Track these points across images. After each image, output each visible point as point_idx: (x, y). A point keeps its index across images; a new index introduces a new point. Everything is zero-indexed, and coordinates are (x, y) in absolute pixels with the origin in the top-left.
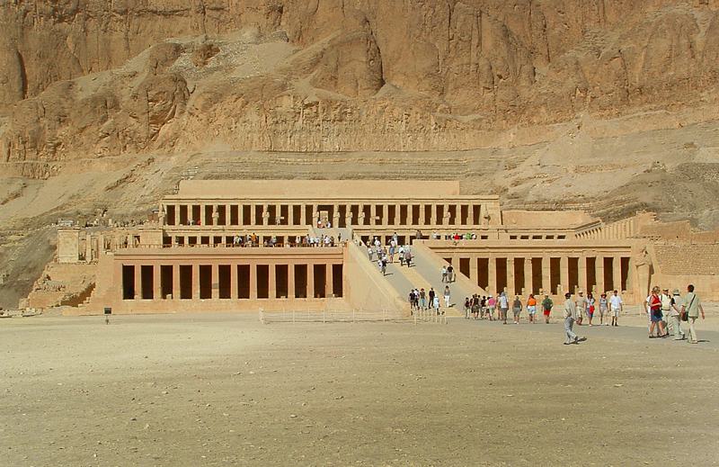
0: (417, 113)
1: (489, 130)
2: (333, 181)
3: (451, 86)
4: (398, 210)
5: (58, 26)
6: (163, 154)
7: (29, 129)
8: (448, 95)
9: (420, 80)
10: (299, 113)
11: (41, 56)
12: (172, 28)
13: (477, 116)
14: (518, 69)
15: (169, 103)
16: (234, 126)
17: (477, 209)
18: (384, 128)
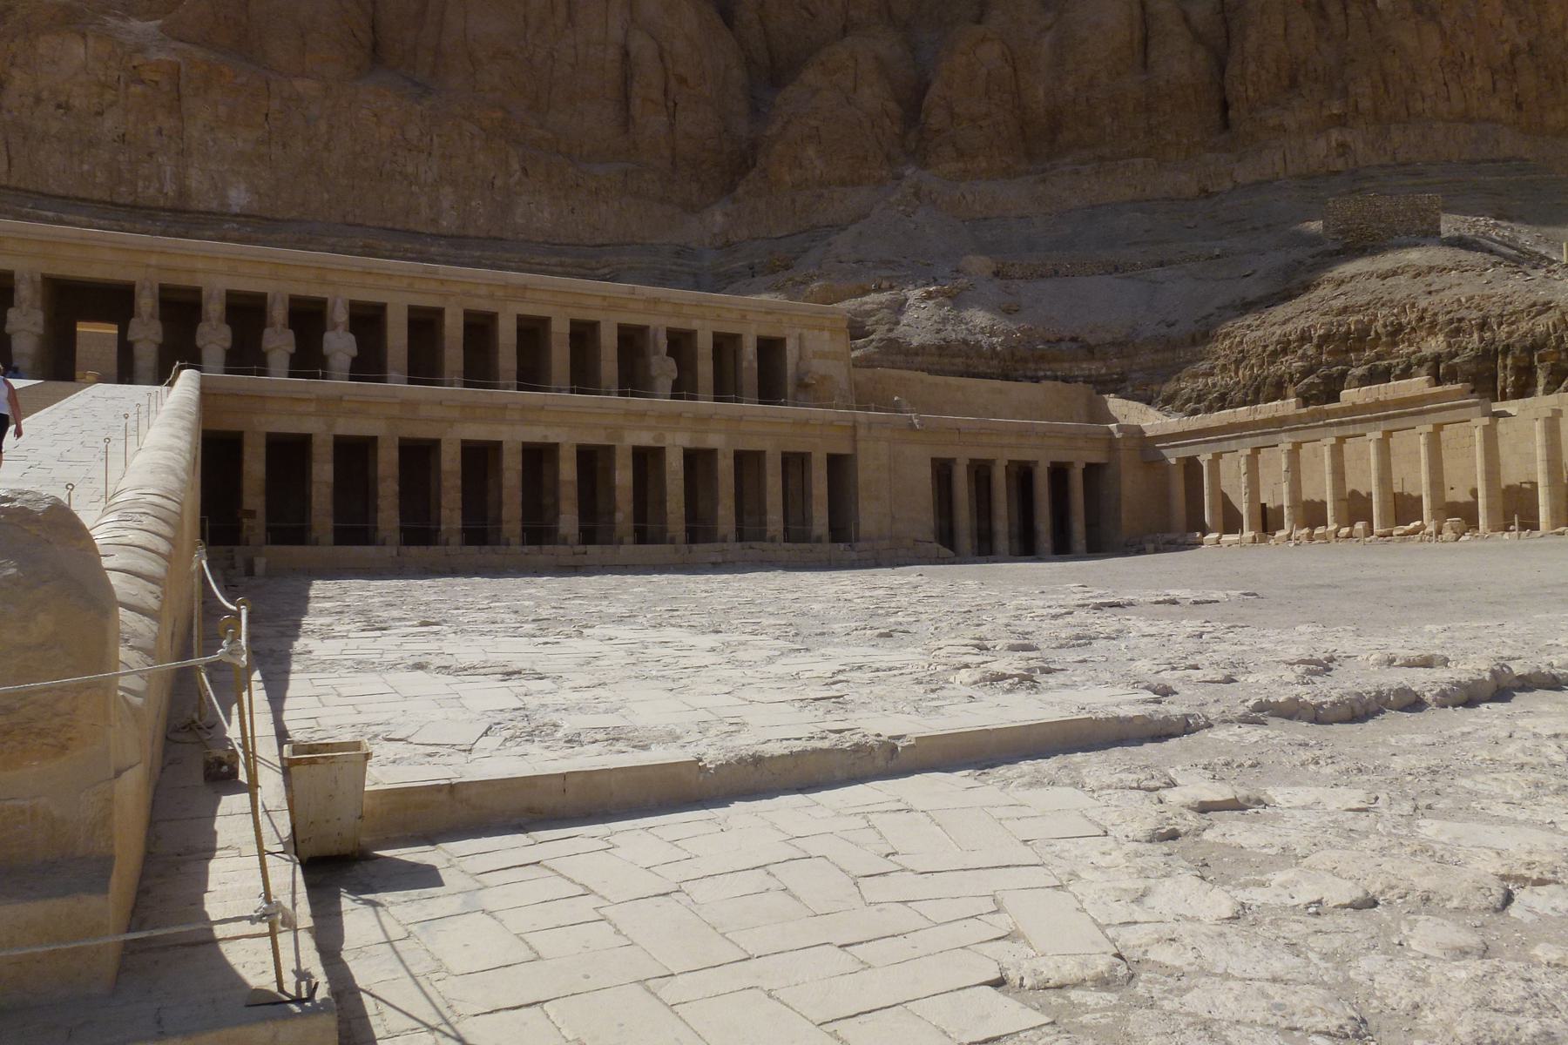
17: (770, 349)
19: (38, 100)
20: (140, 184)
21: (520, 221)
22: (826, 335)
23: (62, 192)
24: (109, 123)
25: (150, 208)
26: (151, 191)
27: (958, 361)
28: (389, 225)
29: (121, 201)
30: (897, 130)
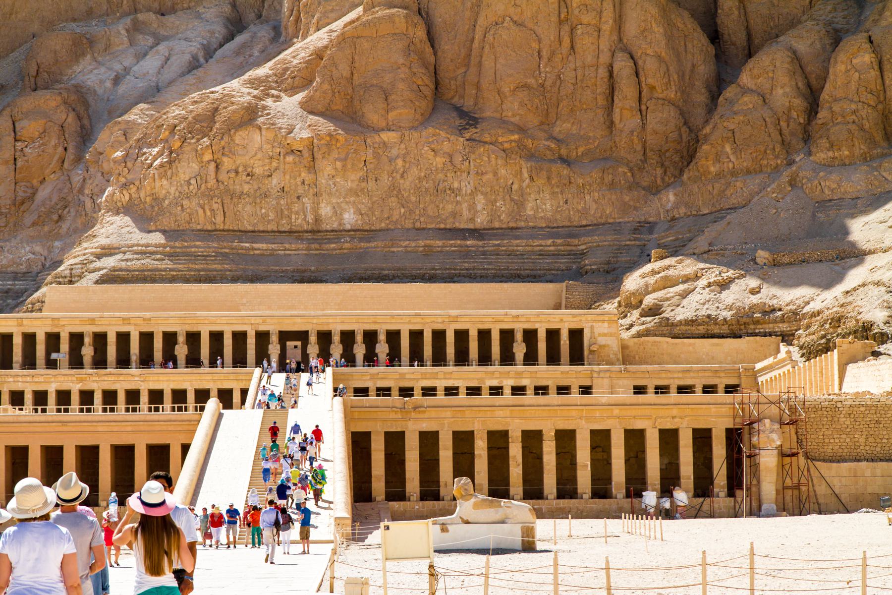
15: (53, 143)
17: (576, 335)
19: (237, 172)
20: (293, 217)
21: (531, 213)
22: (606, 325)
23: (250, 228)
24: (275, 181)
25: (299, 232)
26: (300, 221)
27: (701, 328)
28: (442, 226)
29: (283, 229)
30: (802, 121)
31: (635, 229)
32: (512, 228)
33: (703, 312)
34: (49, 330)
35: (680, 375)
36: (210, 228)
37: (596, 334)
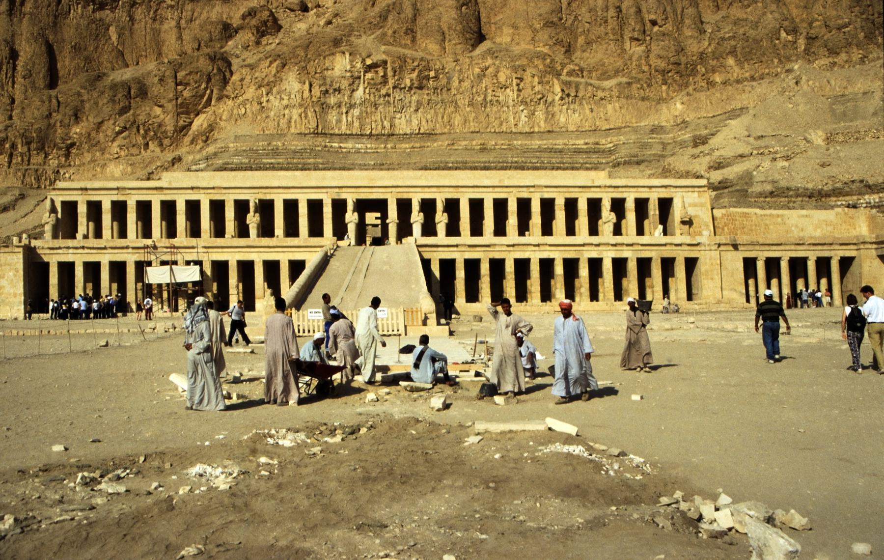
0: (533, 76)
1: (643, 99)
2: (411, 173)
3: (581, 40)
4: (512, 207)
5: (98, 15)
6: (193, 152)
7: (35, 127)
8: (578, 54)
9: (535, 31)
10: (359, 78)
11: (76, 49)
12: (232, 14)
13: (624, 80)
14: (679, 12)
16: (264, 99)
17: (665, 205)
18: (485, 99)
31: (652, 130)
32: (549, 132)
33: (783, 184)
34: (115, 198)
35: (793, 247)
36: (307, 132)
37: (686, 206)
